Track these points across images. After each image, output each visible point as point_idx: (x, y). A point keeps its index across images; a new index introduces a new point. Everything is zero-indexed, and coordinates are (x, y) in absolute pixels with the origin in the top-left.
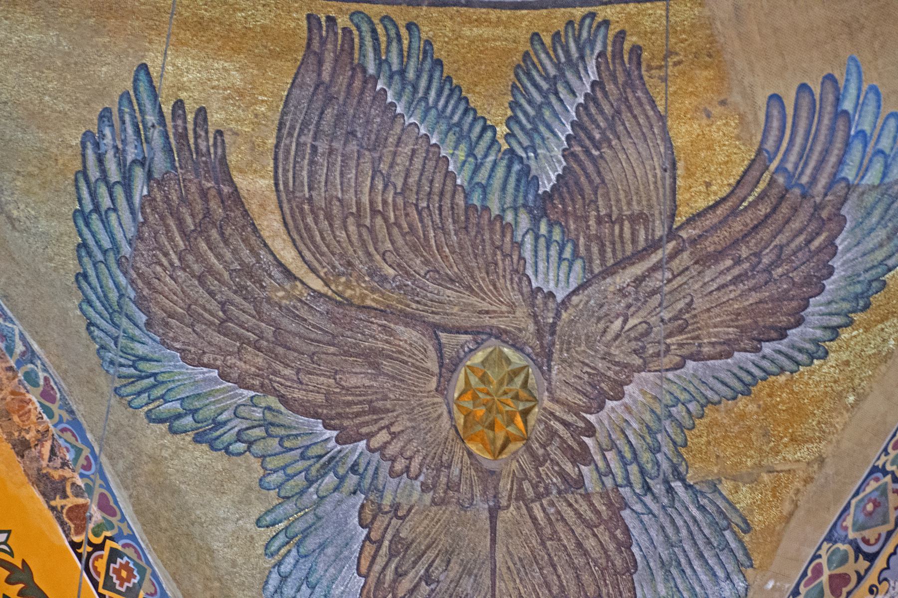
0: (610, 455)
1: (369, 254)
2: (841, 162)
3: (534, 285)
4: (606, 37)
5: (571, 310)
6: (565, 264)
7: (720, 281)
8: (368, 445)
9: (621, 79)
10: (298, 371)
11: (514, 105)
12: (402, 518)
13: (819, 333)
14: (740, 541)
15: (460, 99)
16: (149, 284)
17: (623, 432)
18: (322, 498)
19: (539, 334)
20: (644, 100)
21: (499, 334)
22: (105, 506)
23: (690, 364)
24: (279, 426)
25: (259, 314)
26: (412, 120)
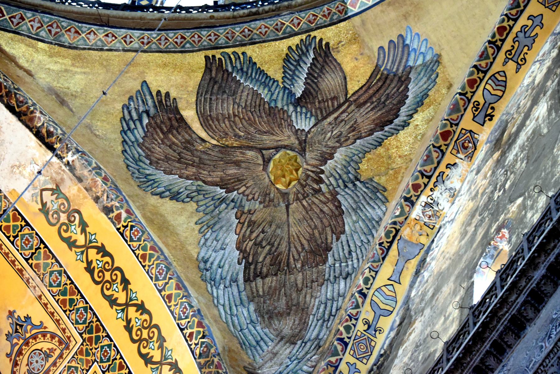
0: (330, 179)
1: (234, 130)
2: (407, 60)
3: (297, 128)
4: (315, 42)
5: (312, 134)
6: (308, 120)
7: (367, 111)
8: (238, 193)
9: (323, 55)
10: (209, 172)
11: (284, 72)
12: (252, 214)
13: (405, 118)
14: (383, 195)
15: (264, 74)
16: (150, 150)
17: (335, 170)
18: (220, 212)
19: (300, 143)
20: (332, 60)
21: (285, 147)
22: (128, 212)
23: (358, 141)
24: (203, 190)
25: (193, 155)
26: (247, 84)
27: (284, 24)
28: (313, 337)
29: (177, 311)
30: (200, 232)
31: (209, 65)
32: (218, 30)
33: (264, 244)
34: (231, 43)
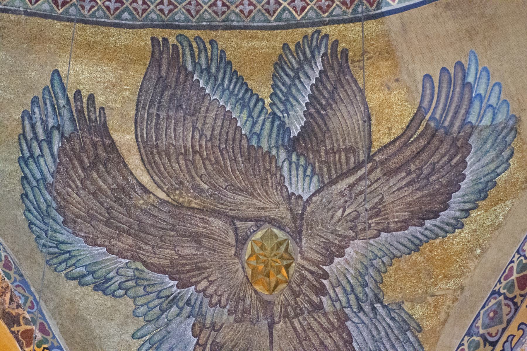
0: (338, 290)
1: (192, 177)
2: (467, 113)
3: (290, 191)
4: (327, 44)
5: (312, 205)
6: (307, 179)
7: (399, 185)
8: (196, 289)
9: (337, 69)
12: (218, 331)
13: (458, 214)
14: (416, 337)
15: (243, 84)
16: (64, 199)
18: (170, 321)
19: (294, 220)
20: (351, 81)
21: (271, 221)
22: (43, 330)
23: (383, 234)
24: (143, 279)
26: (215, 97)
31: (157, 54)
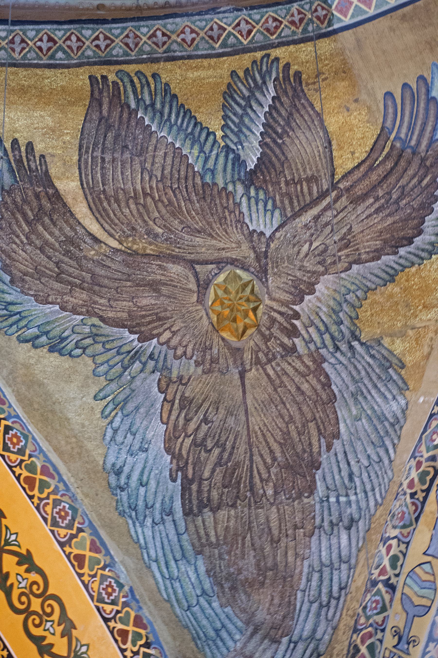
0: (311, 330)
1: (145, 221)
3: (251, 228)
4: (278, 68)
5: (276, 242)
6: (269, 214)
7: (367, 213)
8: (158, 341)
9: (290, 94)
10: (109, 300)
11: (225, 117)
12: (186, 384)
14: (399, 375)
15: (191, 117)
16: (9, 257)
17: (317, 314)
18: (133, 378)
19: (258, 259)
20: (306, 104)
21: (233, 262)
23: (355, 267)
24: (101, 335)
26: (162, 134)
27: (225, 29)
28: (306, 634)
29: (95, 586)
30: (104, 416)
32: (111, 29)
33: (209, 444)
34: (133, 56)
